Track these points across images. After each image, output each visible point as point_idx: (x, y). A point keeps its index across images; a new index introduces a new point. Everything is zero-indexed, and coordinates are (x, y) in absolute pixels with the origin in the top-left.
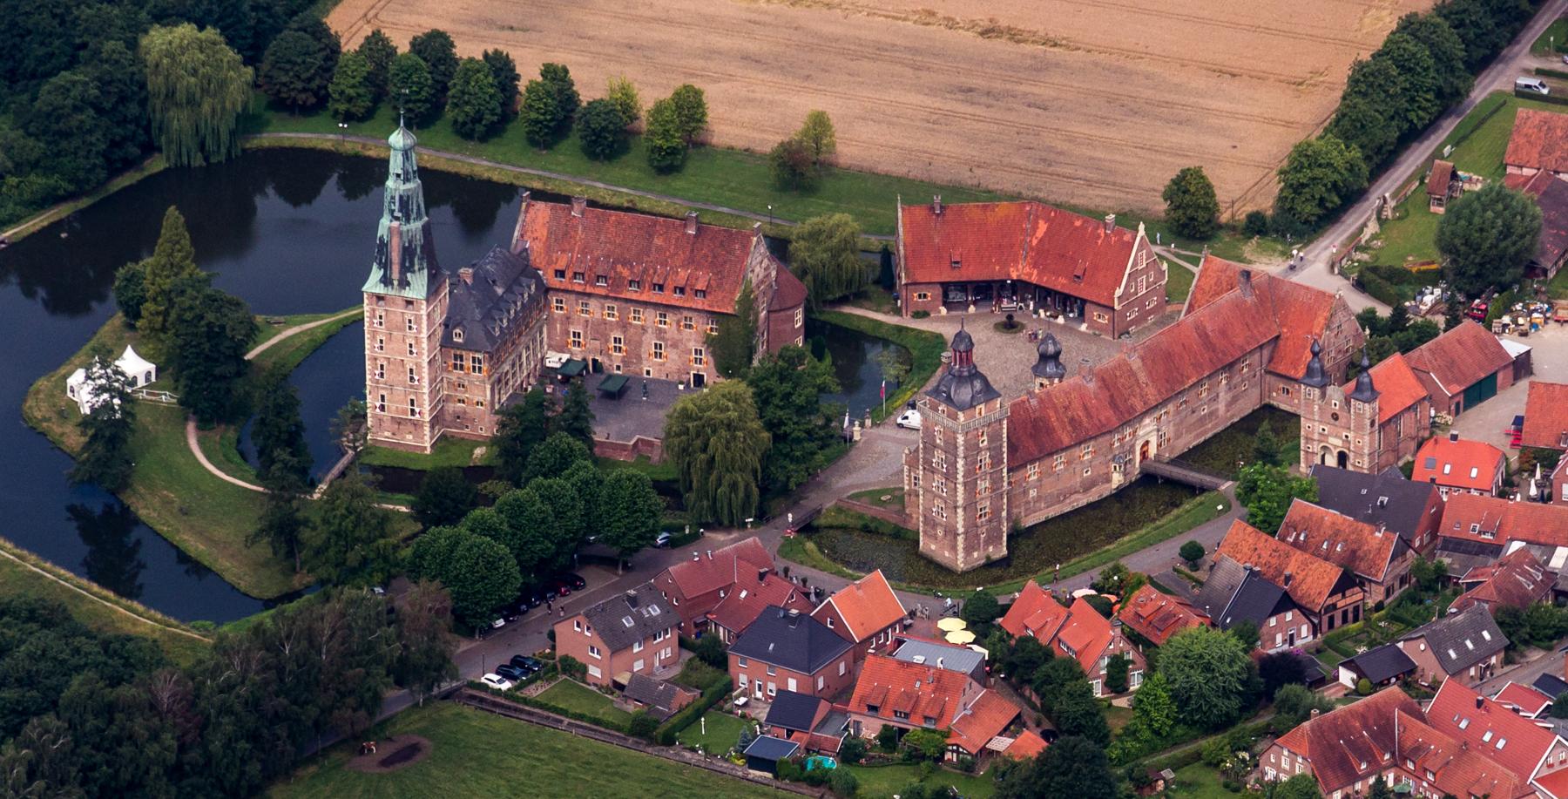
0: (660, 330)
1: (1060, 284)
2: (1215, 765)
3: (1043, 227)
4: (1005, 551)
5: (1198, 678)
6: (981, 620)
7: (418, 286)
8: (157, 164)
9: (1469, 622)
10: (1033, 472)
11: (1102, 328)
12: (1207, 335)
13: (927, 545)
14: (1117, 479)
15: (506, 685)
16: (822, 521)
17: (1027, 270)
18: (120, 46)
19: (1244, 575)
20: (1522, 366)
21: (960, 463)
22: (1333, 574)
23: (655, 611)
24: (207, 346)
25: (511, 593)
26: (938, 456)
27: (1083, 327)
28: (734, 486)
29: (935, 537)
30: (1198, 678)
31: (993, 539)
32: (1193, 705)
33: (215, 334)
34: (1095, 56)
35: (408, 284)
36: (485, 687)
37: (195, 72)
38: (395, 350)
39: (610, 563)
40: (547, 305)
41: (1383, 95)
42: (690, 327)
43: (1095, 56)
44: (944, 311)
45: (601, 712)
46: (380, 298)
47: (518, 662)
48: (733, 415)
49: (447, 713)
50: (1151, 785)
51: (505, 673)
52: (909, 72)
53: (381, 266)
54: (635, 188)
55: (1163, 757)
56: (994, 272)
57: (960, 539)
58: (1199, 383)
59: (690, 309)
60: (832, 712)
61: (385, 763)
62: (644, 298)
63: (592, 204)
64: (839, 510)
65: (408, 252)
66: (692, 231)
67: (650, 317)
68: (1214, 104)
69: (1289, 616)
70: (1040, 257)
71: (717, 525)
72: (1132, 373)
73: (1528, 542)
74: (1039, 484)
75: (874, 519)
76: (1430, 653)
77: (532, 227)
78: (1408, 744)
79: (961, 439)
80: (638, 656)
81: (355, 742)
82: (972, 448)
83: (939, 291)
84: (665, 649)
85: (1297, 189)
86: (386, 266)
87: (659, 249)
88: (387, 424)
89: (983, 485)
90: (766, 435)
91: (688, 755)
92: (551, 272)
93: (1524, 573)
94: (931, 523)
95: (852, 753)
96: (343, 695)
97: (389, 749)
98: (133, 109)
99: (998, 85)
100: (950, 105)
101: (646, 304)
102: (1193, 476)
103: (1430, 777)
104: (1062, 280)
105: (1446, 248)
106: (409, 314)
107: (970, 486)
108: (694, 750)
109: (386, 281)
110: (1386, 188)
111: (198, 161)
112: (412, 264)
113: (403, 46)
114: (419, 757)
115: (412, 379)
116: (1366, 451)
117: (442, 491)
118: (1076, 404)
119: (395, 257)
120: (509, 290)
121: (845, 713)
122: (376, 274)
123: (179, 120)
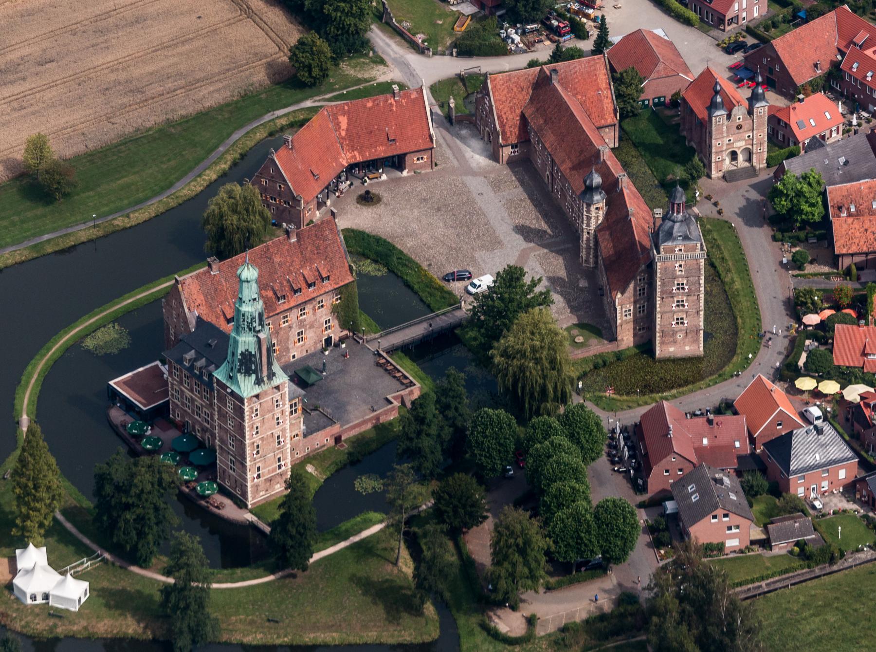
1: (381, 151)
3: (343, 121)
11: (422, 167)
17: (349, 155)
27: (405, 173)
29: (675, 342)
42: (322, 306)
53: (248, 373)
66: (294, 240)
70: (352, 140)
87: (280, 264)
104: (381, 148)
106: (277, 396)
108: (858, 551)
109: (259, 382)
115: (279, 443)
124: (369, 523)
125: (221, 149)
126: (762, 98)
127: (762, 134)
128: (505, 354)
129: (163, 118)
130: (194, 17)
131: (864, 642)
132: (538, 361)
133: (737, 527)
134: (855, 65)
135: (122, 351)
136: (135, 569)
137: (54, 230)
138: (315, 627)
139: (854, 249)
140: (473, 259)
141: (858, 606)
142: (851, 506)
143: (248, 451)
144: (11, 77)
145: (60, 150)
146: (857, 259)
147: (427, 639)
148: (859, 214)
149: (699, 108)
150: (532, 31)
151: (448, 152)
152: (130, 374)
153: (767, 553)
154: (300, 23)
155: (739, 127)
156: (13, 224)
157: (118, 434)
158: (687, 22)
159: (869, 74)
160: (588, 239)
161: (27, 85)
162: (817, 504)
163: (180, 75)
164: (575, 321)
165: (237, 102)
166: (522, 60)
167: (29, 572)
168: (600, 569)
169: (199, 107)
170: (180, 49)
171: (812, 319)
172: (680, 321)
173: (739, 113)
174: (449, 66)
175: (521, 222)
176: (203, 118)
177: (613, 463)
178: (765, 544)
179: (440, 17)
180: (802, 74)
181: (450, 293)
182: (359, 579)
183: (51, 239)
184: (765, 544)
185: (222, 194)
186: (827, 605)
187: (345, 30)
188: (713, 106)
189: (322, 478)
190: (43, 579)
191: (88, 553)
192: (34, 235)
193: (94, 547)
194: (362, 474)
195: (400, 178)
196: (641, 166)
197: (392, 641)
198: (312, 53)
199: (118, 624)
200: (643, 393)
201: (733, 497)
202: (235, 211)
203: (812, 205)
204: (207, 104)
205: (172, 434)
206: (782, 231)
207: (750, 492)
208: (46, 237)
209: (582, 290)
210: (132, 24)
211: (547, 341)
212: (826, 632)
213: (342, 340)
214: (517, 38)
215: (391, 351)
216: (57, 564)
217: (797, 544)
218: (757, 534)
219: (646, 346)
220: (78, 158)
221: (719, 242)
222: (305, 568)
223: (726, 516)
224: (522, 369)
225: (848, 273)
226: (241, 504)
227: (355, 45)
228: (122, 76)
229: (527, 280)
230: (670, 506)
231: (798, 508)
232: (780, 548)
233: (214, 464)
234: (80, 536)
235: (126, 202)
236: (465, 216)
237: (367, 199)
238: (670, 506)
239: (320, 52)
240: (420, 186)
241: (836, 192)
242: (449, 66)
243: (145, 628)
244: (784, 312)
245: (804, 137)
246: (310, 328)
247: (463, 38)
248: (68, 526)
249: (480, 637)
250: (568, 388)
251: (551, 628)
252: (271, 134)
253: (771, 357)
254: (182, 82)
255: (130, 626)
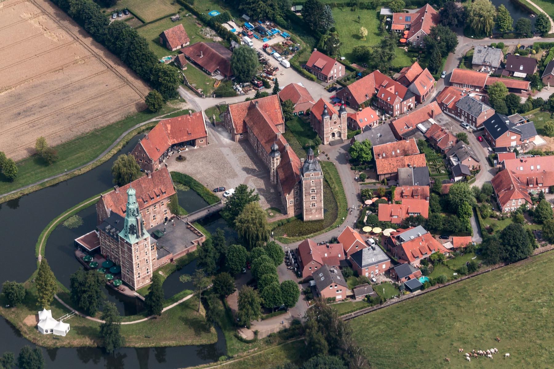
1: (185, 139)
3: (169, 127)
11: (203, 144)
27: (196, 147)
29: (312, 214)
53: (133, 233)
66: (150, 177)
67: (152, 208)
70: (173, 134)
87: (145, 188)
100: (27, 119)
104: (185, 137)
106: (145, 243)
108: (392, 298)
109: (138, 237)
124: (186, 295)
125: (118, 140)
126: (344, 110)
127: (345, 125)
128: (240, 221)
129: (92, 128)
130: (104, 85)
131: (396, 337)
132: (254, 224)
133: (341, 290)
134: (383, 95)
135: (80, 226)
136: (89, 318)
137: (49, 177)
138: (165, 339)
139: (385, 172)
140: (226, 182)
141: (393, 321)
142: (388, 280)
143: (134, 266)
144: (29, 114)
145: (50, 143)
146: (387, 176)
147: (212, 342)
148: (387, 157)
149: (318, 115)
150: (247, 86)
151: (214, 138)
152: (83, 236)
153: (354, 301)
154: (149, 86)
155: (335, 123)
156: (32, 175)
157: (79, 261)
158: (312, 79)
159: (389, 98)
160: (274, 172)
161: (35, 117)
162: (374, 279)
163: (100, 110)
164: (270, 207)
165: (124, 120)
166: (243, 98)
167: (44, 320)
168: (284, 310)
169: (108, 123)
170: (99, 99)
171: (369, 202)
172: (313, 205)
173: (335, 116)
174: (213, 102)
175: (245, 166)
176: (110, 127)
177: (288, 265)
178: (353, 297)
179: (208, 81)
180: (360, 99)
181: (216, 197)
182: (183, 318)
183: (48, 181)
184: (353, 297)
185: (119, 159)
186: (380, 321)
187: (168, 88)
188: (324, 114)
189: (166, 276)
190: (51, 324)
191: (69, 311)
192: (41, 179)
193: (71, 309)
194: (182, 274)
195: (194, 150)
196: (294, 141)
197: (198, 344)
198: (155, 99)
199: (82, 341)
200: (299, 236)
201: (339, 278)
202: (125, 166)
203: (367, 154)
204: (112, 122)
205: (102, 260)
206: (355, 166)
207: (346, 276)
208: (46, 180)
209: (272, 193)
210: (79, 89)
211: (258, 215)
212: (380, 333)
213: (172, 218)
214: (241, 89)
215: (193, 222)
216: (56, 316)
217: (366, 296)
218: (349, 293)
219: (299, 216)
220: (58, 146)
221: (329, 171)
222: (160, 315)
223: (336, 286)
224: (248, 228)
225: (383, 182)
226: (132, 289)
227: (172, 95)
228: (75, 111)
229: (249, 190)
230: (312, 283)
231: (366, 281)
232: (359, 298)
233: (120, 272)
234: (65, 305)
235: (79, 164)
236: (221, 164)
237: (180, 159)
238: (312, 283)
239: (158, 98)
240: (202, 153)
241: (377, 148)
242: (213, 102)
243: (94, 342)
244: (357, 200)
245: (362, 126)
246: (158, 214)
247: (218, 90)
248: (60, 300)
249: (235, 340)
250: (268, 235)
251: (264, 336)
252: (139, 133)
253: (352, 218)
254: (101, 113)
255: (88, 342)
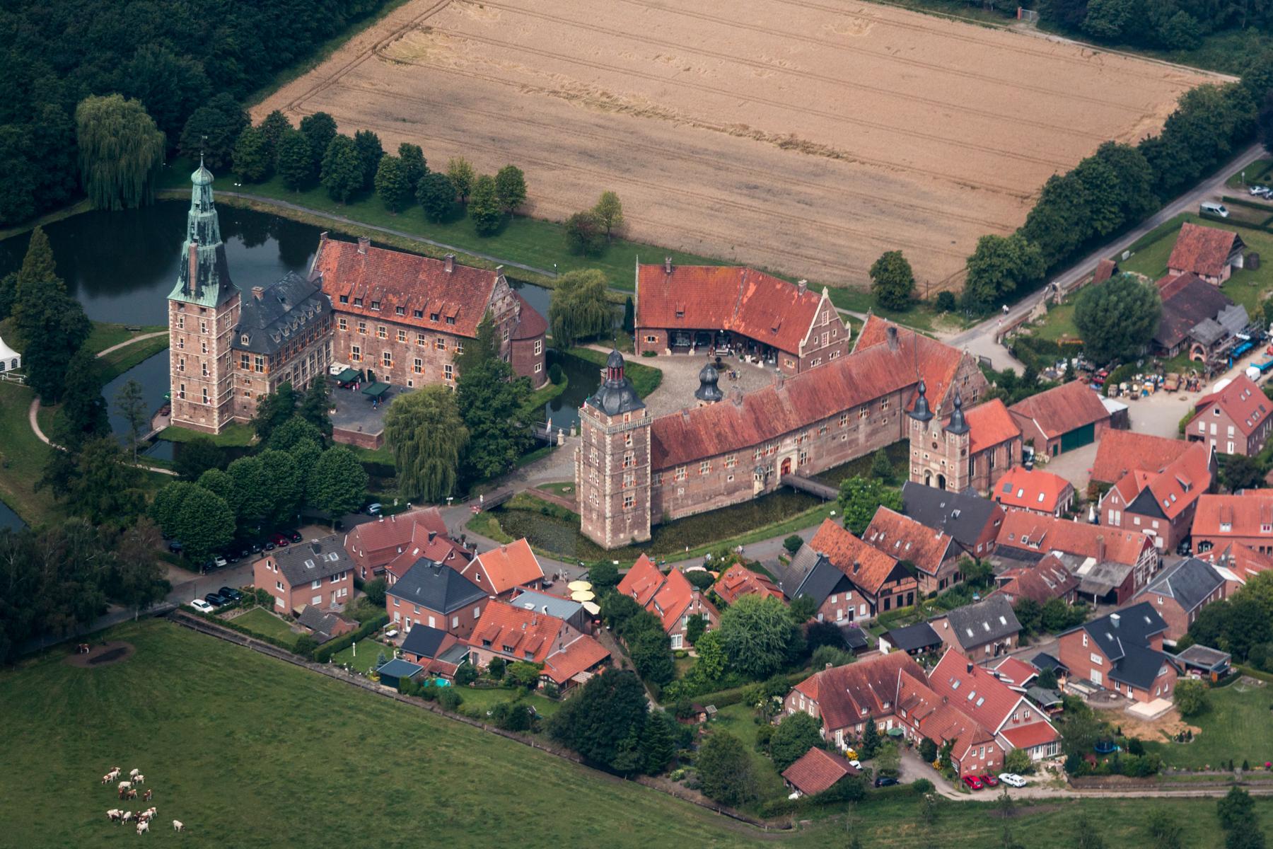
0: (419, 349)
1: (761, 335)
2: (751, 705)
4: (649, 536)
5: (746, 634)
6: (604, 582)
7: (210, 297)
8: (84, 207)
9: (995, 611)
10: (681, 475)
12: (851, 377)
13: (587, 527)
14: (758, 486)
15: (210, 609)
16: (511, 504)
17: (737, 322)
18: (57, 107)
19: (816, 560)
20: (1120, 421)
21: (608, 458)
22: (889, 565)
23: (334, 557)
24: (46, 337)
25: (225, 536)
26: (593, 453)
28: (433, 469)
30: (746, 634)
31: (638, 524)
32: (742, 656)
33: (51, 327)
34: (868, 168)
35: (202, 294)
36: (192, 610)
37: (116, 133)
38: (192, 348)
39: (325, 523)
40: (333, 324)
41: (1068, 204)
42: (442, 347)
43: (868, 168)
44: (669, 352)
45: (279, 635)
46: (181, 305)
47: (225, 592)
48: (433, 410)
49: (155, 628)
50: (695, 716)
51: (211, 600)
52: (711, 170)
54: (457, 246)
55: (710, 696)
56: (710, 323)
57: (608, 522)
58: (839, 415)
59: (442, 332)
60: (456, 645)
61: (93, 661)
62: (407, 321)
63: (374, 244)
64: (527, 496)
65: (203, 269)
66: (449, 270)
67: (412, 337)
68: (946, 208)
69: (849, 596)
70: (749, 312)
71: (417, 502)
72: (778, 402)
73: (1065, 553)
74: (687, 484)
75: (552, 504)
76: (951, 630)
77: (327, 260)
78: (905, 697)
79: (608, 439)
80: (316, 593)
81: (74, 645)
82: (619, 448)
83: (664, 335)
84: (342, 590)
85: (979, 273)
86: (186, 279)
88: (185, 409)
89: (629, 479)
90: (463, 429)
91: (336, 671)
92: (337, 297)
93: (1050, 575)
94: (589, 509)
95: (466, 677)
96: (60, 603)
97: (100, 650)
98: (63, 160)
99: (779, 185)
101: (409, 327)
102: (821, 488)
103: (917, 724)
104: (763, 332)
105: (1082, 327)
107: (617, 478)
108: (342, 667)
109: (186, 291)
110: (1063, 284)
111: (117, 206)
112: (206, 279)
113: (295, 122)
114: (122, 659)
115: (205, 373)
116: (957, 475)
117: (195, 455)
118: (725, 422)
119: (193, 272)
120: (296, 307)
121: (466, 646)
122: (180, 285)
123: (101, 171)
